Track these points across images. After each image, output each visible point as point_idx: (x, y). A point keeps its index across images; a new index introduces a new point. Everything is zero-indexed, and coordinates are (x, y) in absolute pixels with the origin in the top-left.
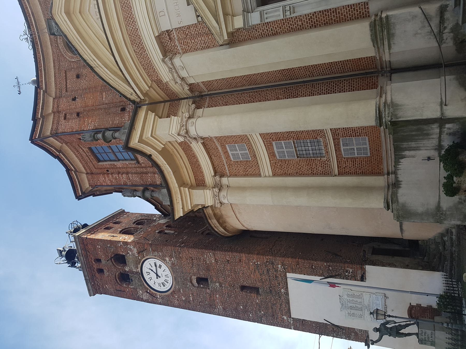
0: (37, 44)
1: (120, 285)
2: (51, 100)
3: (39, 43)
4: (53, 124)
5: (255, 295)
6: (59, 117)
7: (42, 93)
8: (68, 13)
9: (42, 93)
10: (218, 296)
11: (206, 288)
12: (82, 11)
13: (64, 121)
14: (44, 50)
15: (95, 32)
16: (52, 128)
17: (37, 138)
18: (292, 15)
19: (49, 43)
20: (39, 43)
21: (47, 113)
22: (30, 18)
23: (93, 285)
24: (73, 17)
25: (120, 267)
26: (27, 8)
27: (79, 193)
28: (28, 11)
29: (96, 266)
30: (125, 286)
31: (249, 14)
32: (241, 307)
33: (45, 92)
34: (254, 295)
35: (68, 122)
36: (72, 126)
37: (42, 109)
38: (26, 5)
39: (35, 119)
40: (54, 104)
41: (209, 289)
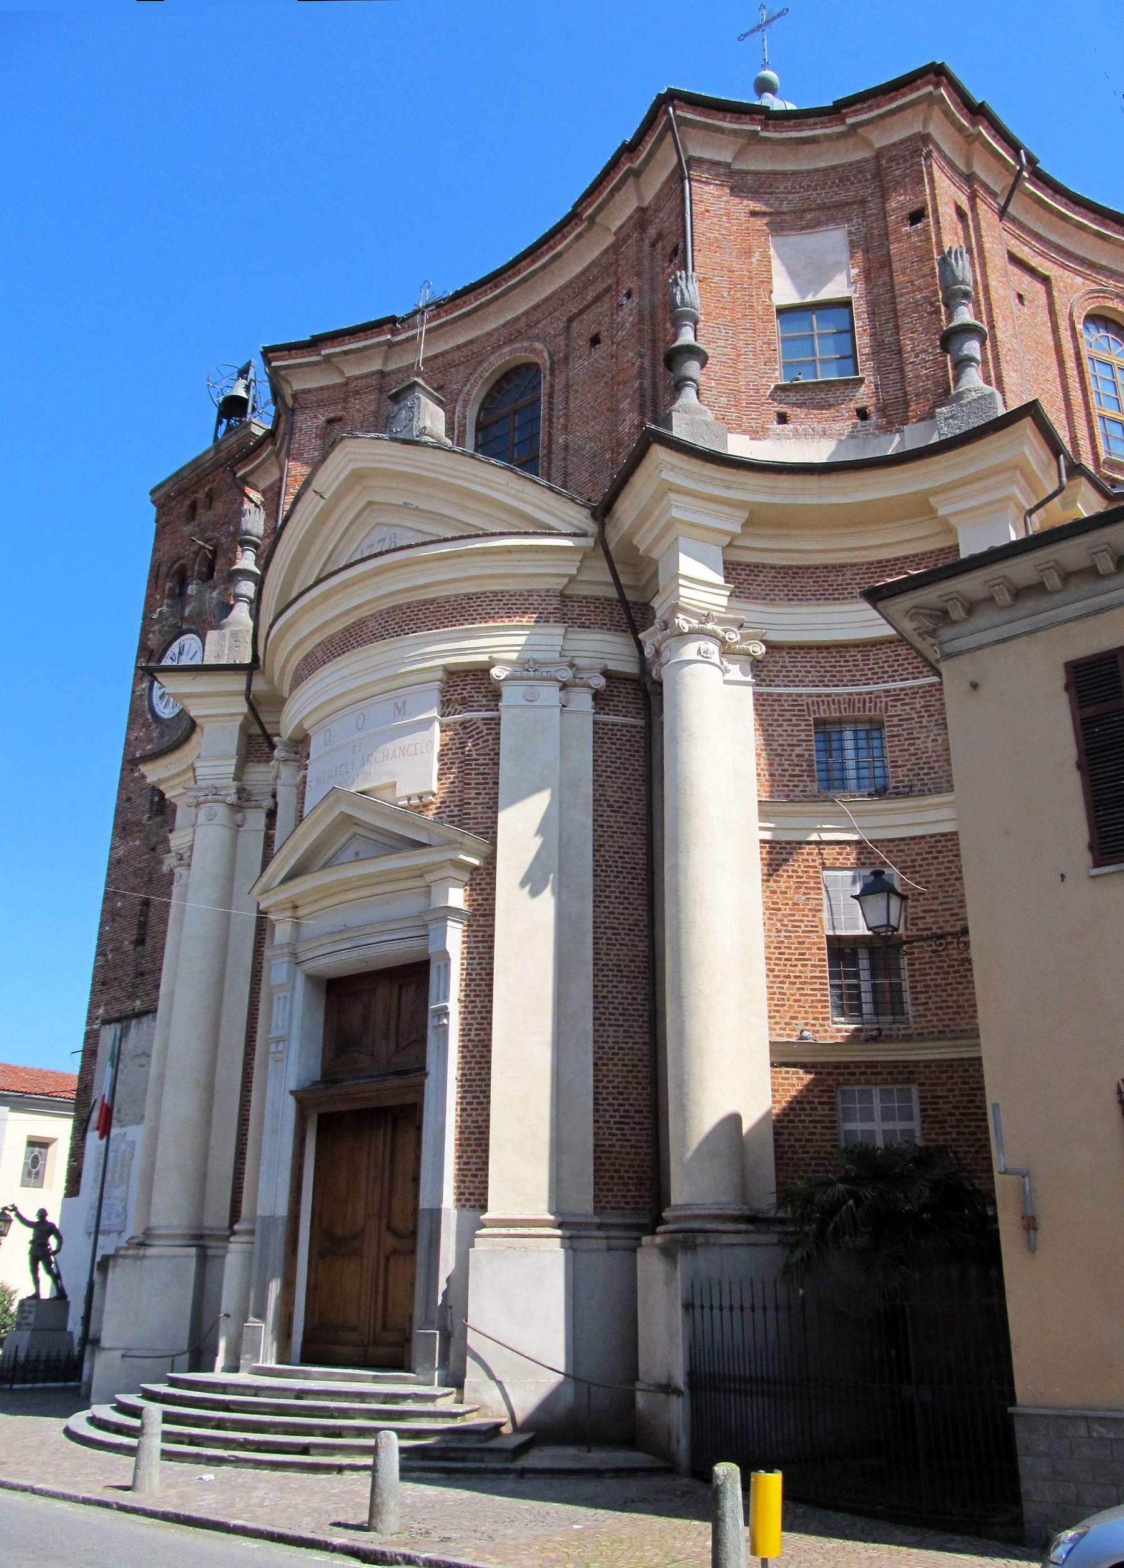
0: (496, 286)
1: (168, 572)
2: (376, 365)
3: (498, 291)
4: (322, 388)
5: (135, 937)
6: (335, 403)
7: (382, 338)
8: (357, 477)
9: (382, 338)
10: (137, 843)
11: (151, 811)
12: (376, 506)
13: (322, 419)
14: (491, 309)
15: (338, 549)
16: (309, 391)
17: (274, 364)
18: (271, 1056)
19: (509, 316)
20: (498, 291)
21: (340, 365)
22: (547, 251)
23: (169, 496)
24: (358, 489)
25: (196, 568)
26: (565, 237)
27: (240, 469)
28: (560, 242)
29: (201, 495)
30: (167, 587)
31: (286, 959)
32: (119, 904)
33: (390, 345)
34: (133, 934)
35: (317, 436)
36: (302, 454)
37: (345, 353)
38: (569, 233)
39: (316, 342)
40: (367, 376)
41: (150, 818)
